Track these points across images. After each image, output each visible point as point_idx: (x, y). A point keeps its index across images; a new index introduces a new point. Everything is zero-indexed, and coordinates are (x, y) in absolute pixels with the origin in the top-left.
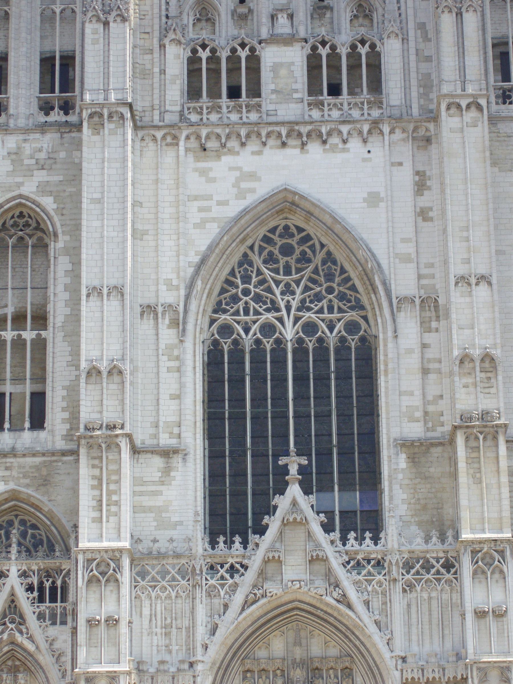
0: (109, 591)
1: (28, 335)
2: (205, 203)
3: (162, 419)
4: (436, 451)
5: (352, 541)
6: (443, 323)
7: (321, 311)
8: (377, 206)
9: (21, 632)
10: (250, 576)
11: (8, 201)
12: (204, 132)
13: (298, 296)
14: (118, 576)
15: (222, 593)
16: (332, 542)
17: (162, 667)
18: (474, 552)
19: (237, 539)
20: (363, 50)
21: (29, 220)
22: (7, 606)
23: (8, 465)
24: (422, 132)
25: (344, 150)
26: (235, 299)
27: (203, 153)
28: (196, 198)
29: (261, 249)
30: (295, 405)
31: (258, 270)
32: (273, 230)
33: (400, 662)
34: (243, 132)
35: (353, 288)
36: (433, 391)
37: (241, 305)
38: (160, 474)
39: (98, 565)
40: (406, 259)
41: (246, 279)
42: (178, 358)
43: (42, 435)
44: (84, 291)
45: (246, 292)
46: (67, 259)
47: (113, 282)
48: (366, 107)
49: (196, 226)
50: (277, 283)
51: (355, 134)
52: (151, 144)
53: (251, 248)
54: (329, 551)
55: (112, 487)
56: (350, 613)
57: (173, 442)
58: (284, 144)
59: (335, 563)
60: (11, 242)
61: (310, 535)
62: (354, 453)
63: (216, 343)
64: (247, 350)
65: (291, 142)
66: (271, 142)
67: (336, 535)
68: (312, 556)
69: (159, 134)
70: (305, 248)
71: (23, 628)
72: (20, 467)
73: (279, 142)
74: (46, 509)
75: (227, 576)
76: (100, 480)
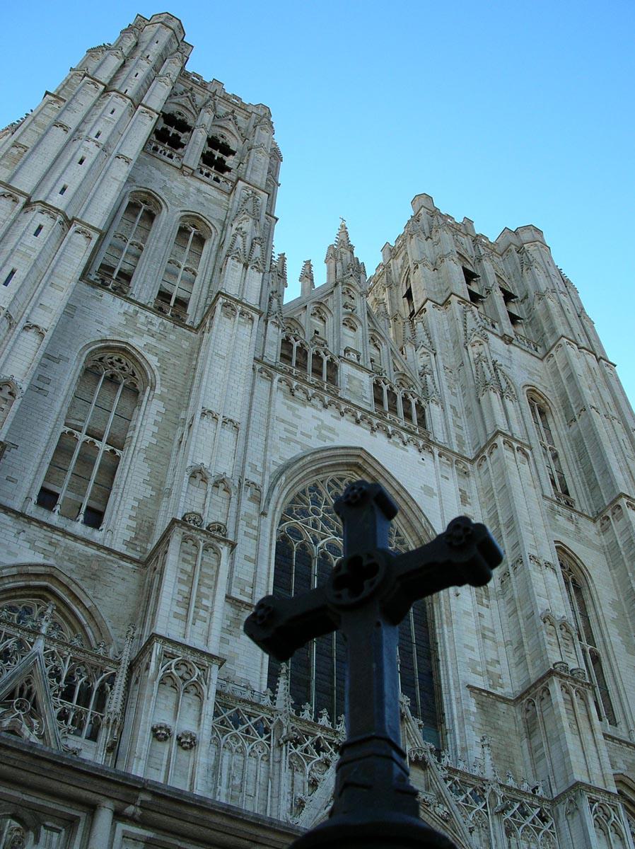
0: (188, 700)
6: (493, 602)
9: (31, 728)
14: (204, 688)
15: (308, 769)
18: (592, 801)
21: (126, 367)
22: (19, 683)
23: (53, 540)
25: (403, 449)
27: (292, 397)
28: (283, 421)
36: (491, 655)
38: (228, 623)
39: (177, 668)
42: (254, 528)
55: (204, 590)
58: (358, 422)
62: (414, 687)
68: (417, 757)
71: (35, 721)
72: (67, 548)
73: (354, 420)
74: (88, 604)
76: (191, 577)
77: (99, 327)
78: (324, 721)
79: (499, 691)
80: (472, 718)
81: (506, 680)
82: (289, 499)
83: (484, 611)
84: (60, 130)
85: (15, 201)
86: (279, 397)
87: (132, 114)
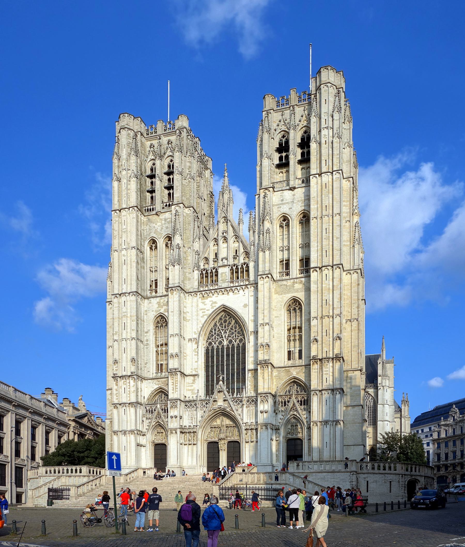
3: (193, 367)
7: (233, 337)
13: (228, 334)
16: (229, 396)
19: (208, 396)
25: (238, 294)
26: (212, 335)
28: (202, 309)
30: (226, 362)
31: (218, 327)
32: (222, 317)
33: (244, 424)
37: (214, 337)
41: (215, 330)
45: (215, 334)
48: (245, 281)
49: (202, 317)
50: (223, 330)
51: (241, 289)
52: (191, 297)
54: (228, 398)
55: (176, 384)
56: (233, 413)
57: (196, 373)
58: (223, 294)
61: (224, 394)
63: (208, 347)
64: (215, 349)
65: (225, 293)
66: (220, 294)
67: (231, 394)
69: (193, 294)
70: (230, 320)
75: (205, 405)
77: (153, 313)
80: (249, 379)
82: (208, 333)
86: (200, 300)
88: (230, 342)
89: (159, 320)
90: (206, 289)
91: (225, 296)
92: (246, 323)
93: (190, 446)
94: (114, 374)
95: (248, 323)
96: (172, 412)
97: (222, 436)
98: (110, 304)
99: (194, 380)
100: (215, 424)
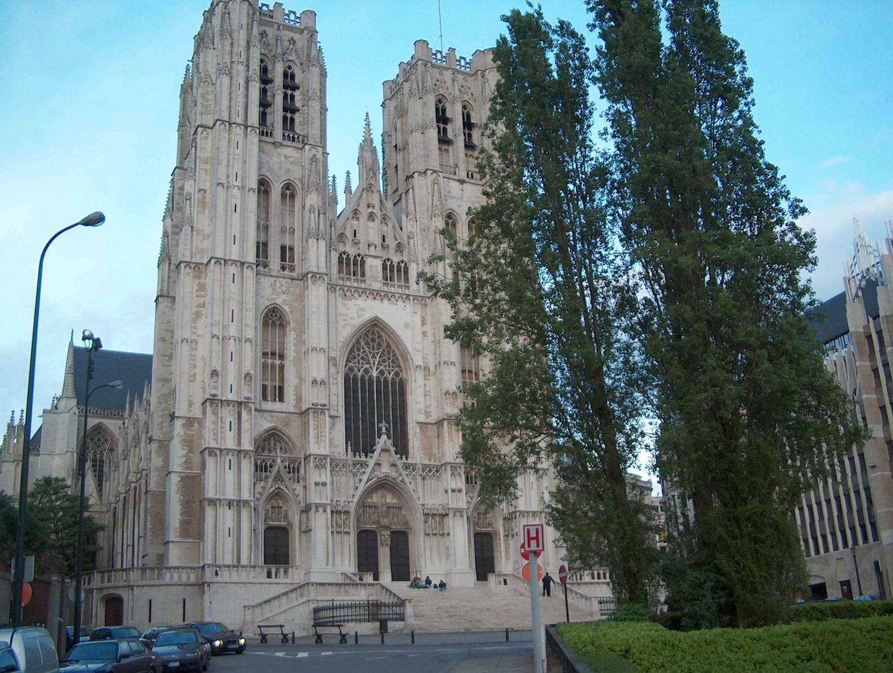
0: (323, 470)
1: (277, 362)
2: (346, 318)
4: (430, 426)
5: (404, 459)
8: (407, 328)
10: (369, 470)
11: (270, 305)
12: (346, 289)
17: (338, 503)
18: (451, 467)
20: (403, 265)
24: (424, 301)
25: (397, 304)
26: (354, 358)
28: (342, 315)
29: (364, 339)
34: (360, 291)
35: (397, 359)
36: (428, 403)
40: (418, 350)
42: (336, 379)
43: (284, 404)
44: (310, 349)
45: (359, 355)
46: (294, 333)
47: (321, 347)
49: (342, 326)
53: (361, 337)
58: (375, 298)
59: (400, 466)
60: (270, 322)
65: (378, 298)
76: (318, 427)
78: (363, 458)
79: (429, 420)
81: (432, 414)
83: (427, 382)
84: (220, 186)
85: (220, 264)
86: (339, 300)
87: (246, 135)
88: (382, 373)
89: (269, 314)
90: (348, 283)
91: (378, 302)
92: (409, 353)
93: (339, 535)
94: (214, 395)
95: (411, 352)
96: (315, 476)
97: (385, 521)
98: (188, 267)
99: (333, 425)
100: (369, 500)
